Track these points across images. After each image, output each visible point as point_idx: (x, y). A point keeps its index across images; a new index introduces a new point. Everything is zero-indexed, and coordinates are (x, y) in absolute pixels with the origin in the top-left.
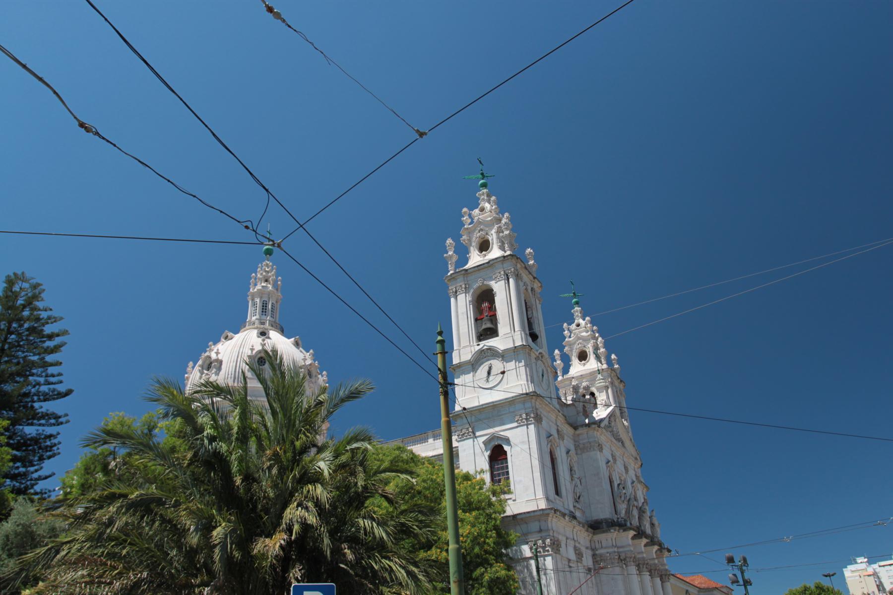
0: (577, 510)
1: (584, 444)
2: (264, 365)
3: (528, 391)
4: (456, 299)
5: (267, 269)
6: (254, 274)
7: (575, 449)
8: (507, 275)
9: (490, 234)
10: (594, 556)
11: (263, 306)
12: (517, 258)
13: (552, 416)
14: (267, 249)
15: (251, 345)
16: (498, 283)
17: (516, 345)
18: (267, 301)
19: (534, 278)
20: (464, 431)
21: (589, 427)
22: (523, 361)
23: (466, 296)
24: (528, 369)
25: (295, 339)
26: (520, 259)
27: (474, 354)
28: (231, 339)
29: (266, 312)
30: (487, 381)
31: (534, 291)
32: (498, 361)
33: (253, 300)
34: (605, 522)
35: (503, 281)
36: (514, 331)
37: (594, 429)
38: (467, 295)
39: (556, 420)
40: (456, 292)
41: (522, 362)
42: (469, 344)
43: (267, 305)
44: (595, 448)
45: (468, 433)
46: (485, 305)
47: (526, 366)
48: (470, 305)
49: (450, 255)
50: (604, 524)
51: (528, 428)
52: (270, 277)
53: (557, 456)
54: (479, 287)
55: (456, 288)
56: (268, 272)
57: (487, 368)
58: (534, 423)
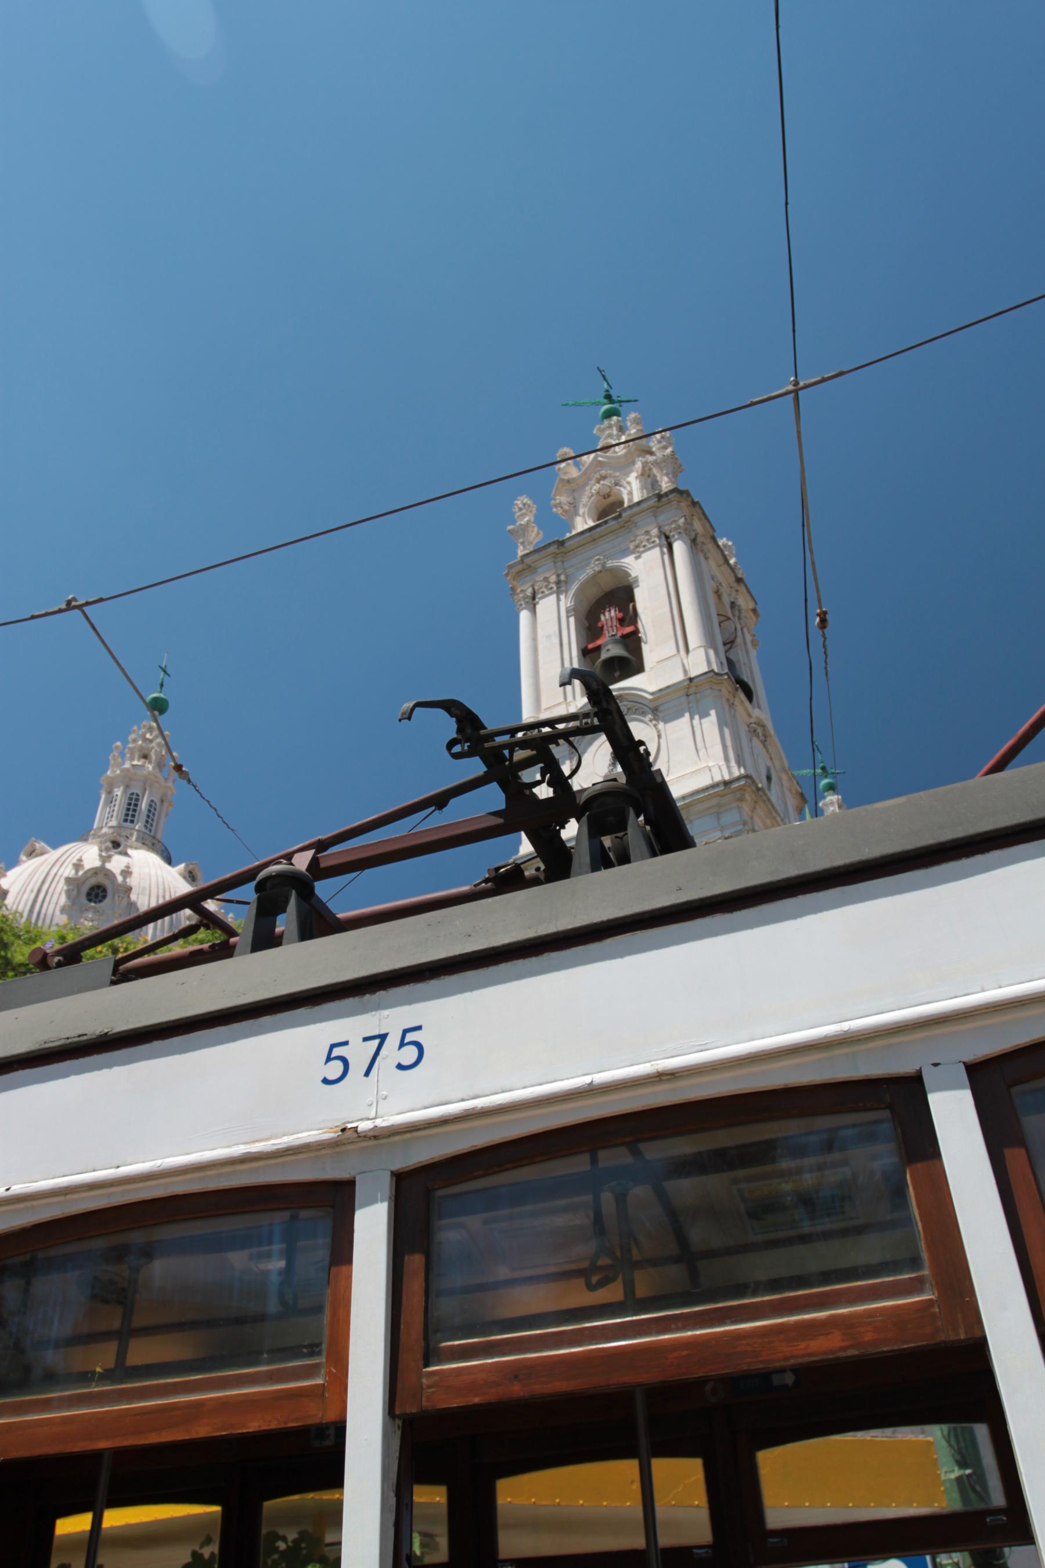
2: (100, 901)
3: (727, 777)
4: (533, 611)
5: (148, 736)
6: (118, 743)
8: (667, 537)
9: (624, 483)
11: (129, 804)
12: (695, 504)
14: (155, 699)
15: (78, 857)
16: (643, 555)
17: (693, 674)
19: (739, 580)
22: (713, 712)
23: (558, 600)
24: (727, 731)
25: (187, 866)
26: (701, 508)
28: (42, 854)
29: (133, 816)
31: (739, 611)
33: (110, 792)
35: (657, 550)
36: (687, 651)
38: (562, 597)
40: (534, 598)
41: (708, 715)
42: (562, 699)
43: (139, 803)
46: (609, 616)
47: (721, 724)
48: (568, 617)
49: (521, 525)
52: (153, 748)
55: (533, 586)
56: (151, 741)
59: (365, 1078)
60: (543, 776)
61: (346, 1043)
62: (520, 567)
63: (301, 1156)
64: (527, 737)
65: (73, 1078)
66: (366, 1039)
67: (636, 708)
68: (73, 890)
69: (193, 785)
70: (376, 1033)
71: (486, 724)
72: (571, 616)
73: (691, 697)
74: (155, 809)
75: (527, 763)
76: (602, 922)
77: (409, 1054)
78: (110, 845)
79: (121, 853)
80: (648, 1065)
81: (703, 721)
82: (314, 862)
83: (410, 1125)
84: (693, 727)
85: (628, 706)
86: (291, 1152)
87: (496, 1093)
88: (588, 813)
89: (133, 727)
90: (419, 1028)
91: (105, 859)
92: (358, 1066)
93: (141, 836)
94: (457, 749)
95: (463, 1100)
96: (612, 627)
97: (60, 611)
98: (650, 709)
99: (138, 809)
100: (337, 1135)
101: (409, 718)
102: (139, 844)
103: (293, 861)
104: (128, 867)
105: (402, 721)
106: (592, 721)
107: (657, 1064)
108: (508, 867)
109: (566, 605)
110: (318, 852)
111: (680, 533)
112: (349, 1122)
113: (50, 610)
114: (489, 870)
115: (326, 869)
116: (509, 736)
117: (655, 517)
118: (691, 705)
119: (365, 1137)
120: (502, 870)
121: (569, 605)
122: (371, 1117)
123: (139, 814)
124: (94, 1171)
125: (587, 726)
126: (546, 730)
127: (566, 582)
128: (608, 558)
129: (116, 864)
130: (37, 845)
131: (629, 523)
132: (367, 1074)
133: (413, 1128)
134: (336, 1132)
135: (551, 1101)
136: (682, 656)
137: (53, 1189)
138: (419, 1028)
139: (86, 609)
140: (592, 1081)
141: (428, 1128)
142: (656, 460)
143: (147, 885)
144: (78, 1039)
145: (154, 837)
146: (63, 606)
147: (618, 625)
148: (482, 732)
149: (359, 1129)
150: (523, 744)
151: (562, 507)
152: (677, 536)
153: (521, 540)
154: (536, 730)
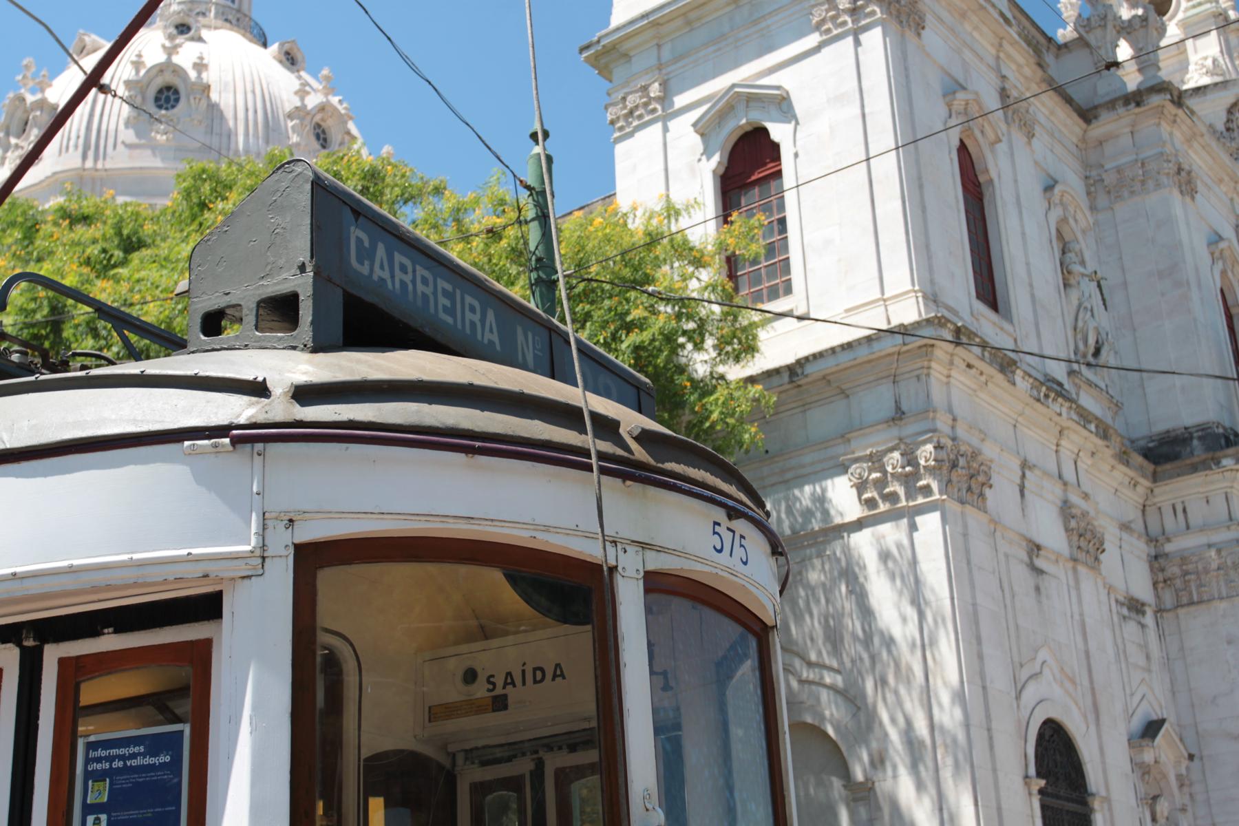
0: (1084, 387)
1: (1118, 172)
2: (173, 107)
7: (1089, 193)
10: (1157, 560)
13: (976, 34)
15: (136, 52)
20: (632, 100)
21: (1138, 104)
25: (282, 45)
34: (1200, 438)
37: (1160, 110)
39: (998, 58)
44: (1164, 180)
45: (646, 105)
50: (1195, 442)
51: (857, 43)
53: (993, 174)
58: (881, 22)
68: (136, 97)
78: (173, 30)
79: (192, 39)
91: (171, 51)
93: (221, 11)
102: (220, 23)
104: (201, 58)
129: (186, 56)
130: (86, 38)
143: (230, 78)
145: (239, 11)
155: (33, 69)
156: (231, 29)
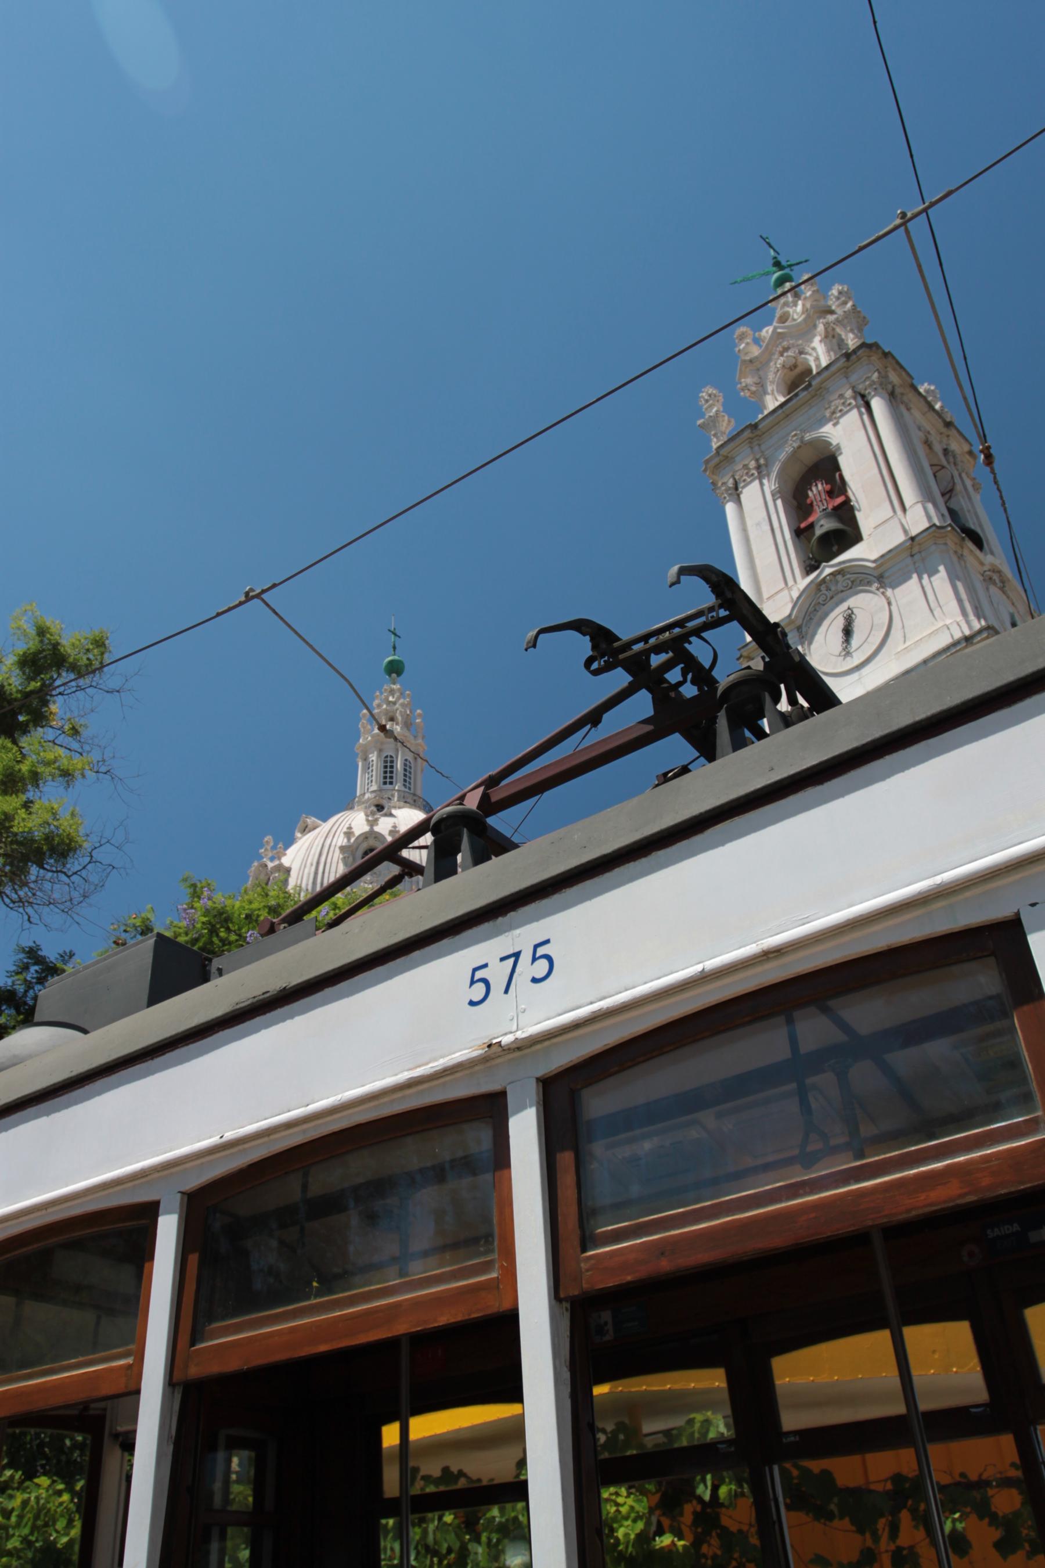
3: (967, 633)
4: (738, 502)
5: (391, 699)
8: (863, 396)
11: (386, 767)
12: (886, 355)
14: (391, 662)
15: (347, 825)
16: (842, 421)
17: (914, 533)
18: (394, 756)
19: (948, 424)
22: (941, 568)
23: (762, 484)
24: (959, 585)
26: (894, 358)
27: (799, 598)
28: (314, 828)
29: (391, 777)
30: (847, 653)
31: (954, 457)
32: (870, 595)
33: (365, 759)
35: (855, 412)
36: (904, 509)
38: (765, 481)
40: (736, 489)
42: (782, 585)
43: (395, 764)
46: (817, 490)
47: (953, 578)
48: (774, 501)
49: (711, 417)
52: (397, 710)
54: (794, 456)
55: (733, 477)
56: (394, 703)
57: (840, 623)
59: (506, 995)
60: (684, 674)
61: (486, 966)
62: (716, 460)
63: (458, 1075)
64: (659, 641)
65: (263, 1032)
66: (502, 959)
67: (861, 579)
68: (348, 857)
69: (400, 742)
70: (511, 952)
71: (620, 636)
72: (777, 499)
73: (916, 557)
74: (410, 767)
75: (668, 666)
76: (701, 814)
77: (542, 966)
78: (374, 809)
79: (386, 815)
80: (754, 945)
81: (933, 579)
82: (485, 799)
83: (546, 1033)
84: (923, 587)
85: (852, 579)
86: (449, 1072)
87: (620, 992)
88: (725, 706)
89: (375, 693)
90: (547, 942)
91: (372, 823)
92: (498, 986)
93: (402, 795)
94: (595, 666)
95: (591, 1003)
96: (821, 501)
97: (241, 604)
98: (875, 577)
99: (394, 770)
100: (484, 1051)
101: (534, 646)
102: (402, 804)
103: (464, 803)
104: (395, 827)
105: (529, 650)
106: (718, 614)
107: (762, 944)
108: (676, 771)
109: (770, 487)
110: (488, 787)
111: (876, 389)
112: (495, 1038)
113: (231, 605)
114: (657, 776)
115: (497, 802)
116: (643, 643)
117: (847, 378)
118: (917, 565)
119: (509, 1049)
120: (670, 775)
121: (773, 487)
122: (513, 1031)
123: (396, 774)
124: (289, 1111)
125: (713, 619)
126: (677, 630)
127: (766, 465)
128: (804, 431)
130: (308, 820)
131: (821, 390)
132: (506, 991)
133: (550, 1036)
134: (483, 1049)
135: (670, 992)
136: (899, 517)
137: (257, 1132)
138: (547, 942)
139: (264, 596)
140: (703, 969)
141: (564, 1033)
142: (837, 318)
144: (261, 997)
145: (414, 795)
146: (243, 598)
147: (828, 498)
148: (616, 645)
149: (503, 1043)
150: (658, 649)
151: (749, 390)
152: (873, 393)
153: (713, 433)
154: (668, 633)
155: (272, 844)
156: (410, 808)
